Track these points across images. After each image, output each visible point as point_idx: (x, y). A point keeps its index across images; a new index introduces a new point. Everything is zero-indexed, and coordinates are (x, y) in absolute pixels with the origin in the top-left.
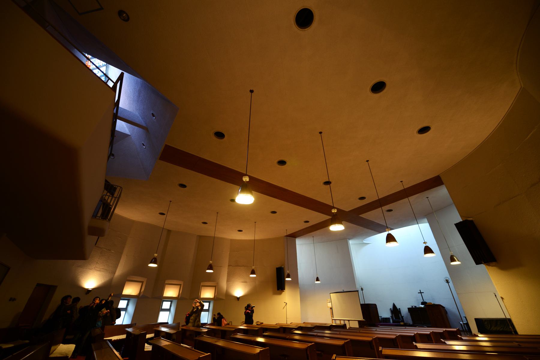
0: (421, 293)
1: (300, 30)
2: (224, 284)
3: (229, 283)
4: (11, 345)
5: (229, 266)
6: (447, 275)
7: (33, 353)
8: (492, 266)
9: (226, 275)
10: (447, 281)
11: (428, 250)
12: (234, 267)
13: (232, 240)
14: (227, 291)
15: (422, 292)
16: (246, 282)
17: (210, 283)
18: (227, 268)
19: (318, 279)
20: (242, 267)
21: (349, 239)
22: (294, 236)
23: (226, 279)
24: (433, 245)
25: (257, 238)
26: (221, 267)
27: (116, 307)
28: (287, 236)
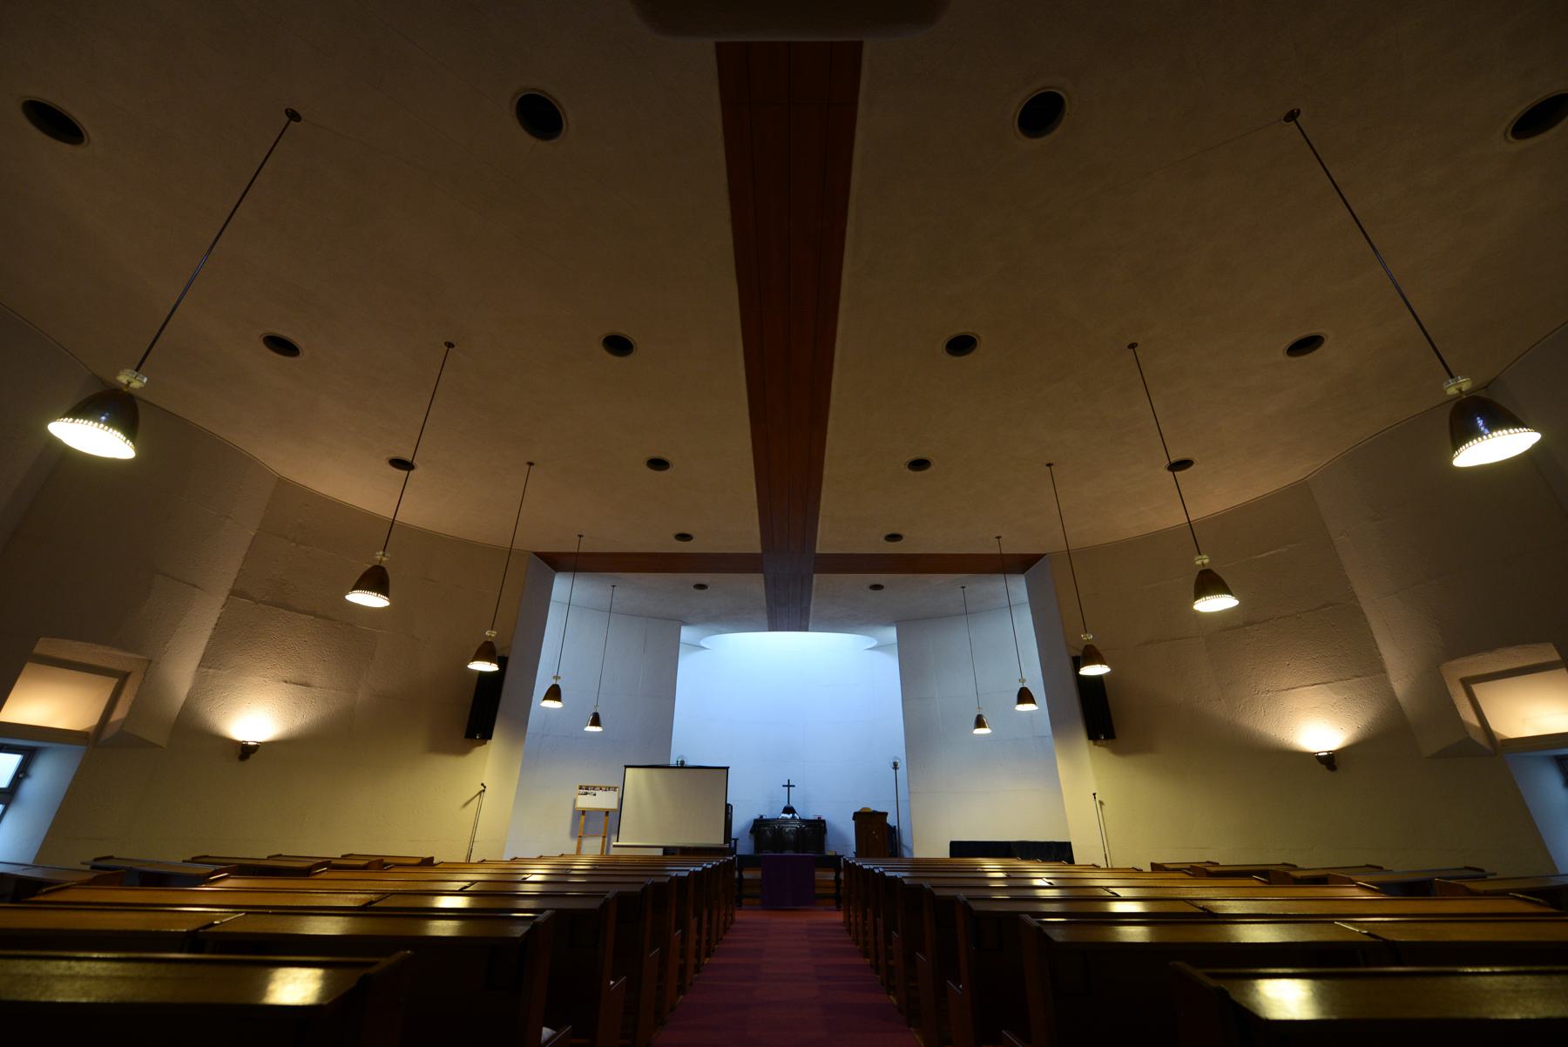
0: (789, 786)
1: (1038, 90)
2: (181, 675)
3: (211, 671)
4: (1181, 964)
5: (233, 593)
6: (900, 753)
7: (1471, 965)
8: (1100, 746)
9: (208, 633)
10: (895, 766)
11: (1025, 696)
12: (263, 606)
13: (283, 484)
14: (187, 709)
15: (791, 788)
16: (306, 685)
17: (100, 649)
18: (223, 599)
19: (596, 721)
20: (304, 616)
21: (686, 624)
22: (558, 562)
23: (201, 652)
24: (1038, 690)
25: (407, 516)
26: (195, 586)
27: (187, 709)
28: (536, 554)
